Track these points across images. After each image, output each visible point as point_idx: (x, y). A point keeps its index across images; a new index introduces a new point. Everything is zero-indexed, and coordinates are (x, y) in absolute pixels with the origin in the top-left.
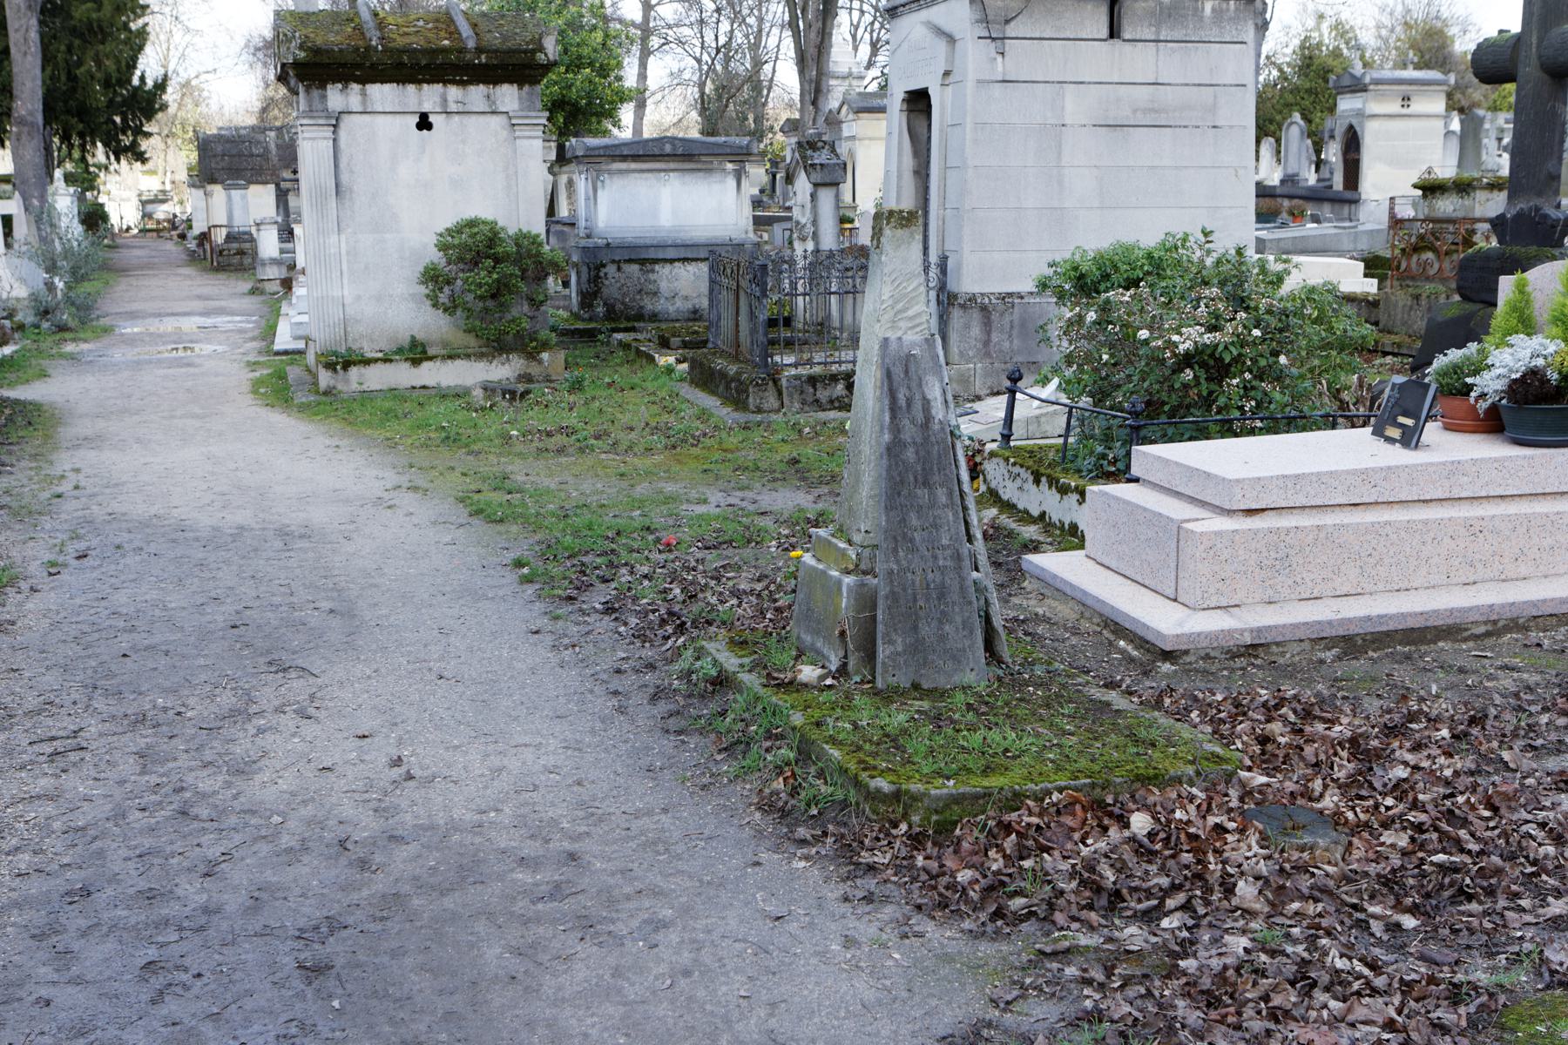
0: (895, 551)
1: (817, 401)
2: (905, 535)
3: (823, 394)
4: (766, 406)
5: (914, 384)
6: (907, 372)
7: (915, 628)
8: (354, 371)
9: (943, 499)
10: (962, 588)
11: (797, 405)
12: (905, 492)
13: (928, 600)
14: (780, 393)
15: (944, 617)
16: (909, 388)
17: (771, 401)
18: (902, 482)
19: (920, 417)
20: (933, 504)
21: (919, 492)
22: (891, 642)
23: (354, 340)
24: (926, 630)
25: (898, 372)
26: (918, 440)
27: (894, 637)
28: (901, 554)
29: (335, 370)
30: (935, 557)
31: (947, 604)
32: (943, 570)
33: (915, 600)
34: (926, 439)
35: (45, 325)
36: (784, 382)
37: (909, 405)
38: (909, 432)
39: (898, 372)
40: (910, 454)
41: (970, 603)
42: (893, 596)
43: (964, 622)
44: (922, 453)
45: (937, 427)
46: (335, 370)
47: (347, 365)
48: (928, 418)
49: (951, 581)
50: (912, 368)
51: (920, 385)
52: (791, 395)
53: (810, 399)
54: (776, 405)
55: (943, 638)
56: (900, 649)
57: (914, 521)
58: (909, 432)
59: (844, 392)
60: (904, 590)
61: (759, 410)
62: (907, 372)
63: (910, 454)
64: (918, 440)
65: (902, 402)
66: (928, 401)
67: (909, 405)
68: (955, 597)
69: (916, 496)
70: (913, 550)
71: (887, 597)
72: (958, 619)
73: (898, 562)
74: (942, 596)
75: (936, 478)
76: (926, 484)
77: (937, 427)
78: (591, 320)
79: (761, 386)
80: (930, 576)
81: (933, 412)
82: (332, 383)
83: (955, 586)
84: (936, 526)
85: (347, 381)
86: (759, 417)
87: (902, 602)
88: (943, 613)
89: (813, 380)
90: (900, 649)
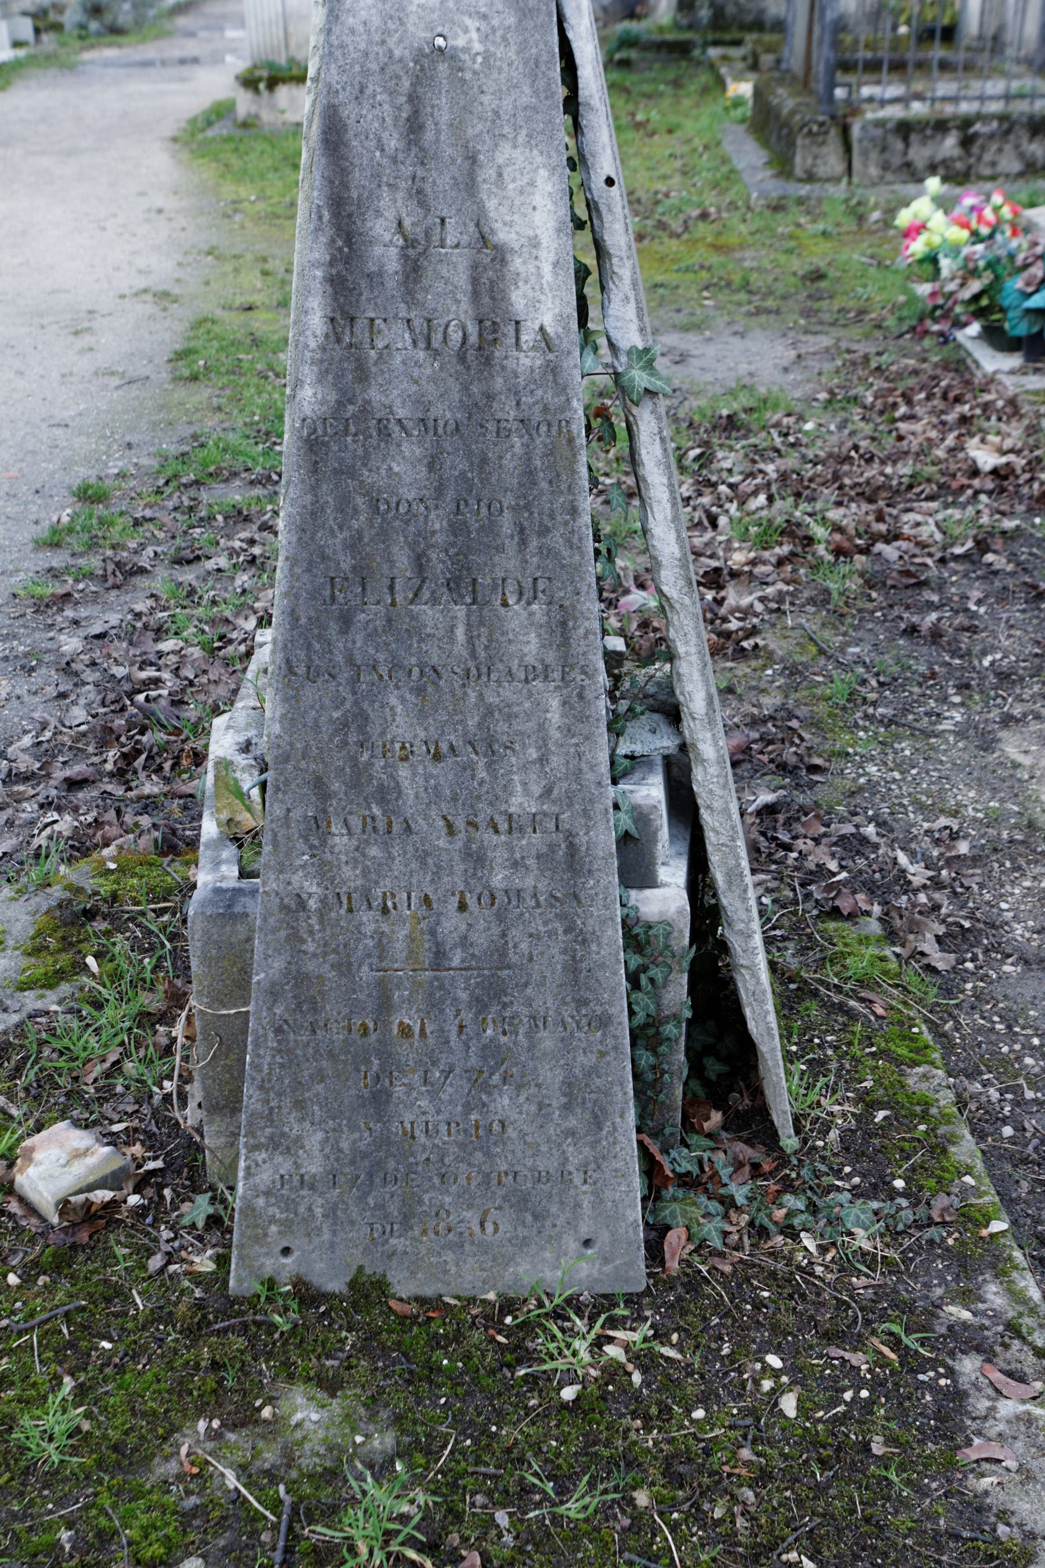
0: (317, 828)
1: (908, 165)
2: (358, 776)
3: (919, 154)
4: (821, 171)
5: (441, 181)
6: (414, 127)
7: (379, 1100)
8: (283, 92)
9: (530, 646)
10: (577, 972)
11: (874, 171)
12: (373, 613)
13: (434, 1007)
14: (848, 148)
15: (494, 1067)
16: (419, 196)
17: (832, 161)
18: (363, 576)
19: (458, 316)
20: (481, 667)
21: (429, 614)
22: (278, 1144)
23: (299, 46)
24: (415, 1107)
25: (376, 125)
26: (444, 412)
27: (293, 1127)
28: (340, 841)
29: (257, 90)
30: (477, 859)
31: (508, 1025)
32: (502, 905)
33: (385, 1005)
34: (477, 409)
35: (94, 26)
36: (856, 131)
37: (413, 269)
38: (406, 378)
39: (376, 125)
40: (403, 468)
41: (604, 1022)
42: (301, 991)
43: (569, 1087)
44: (455, 464)
45: (526, 361)
46: (257, 90)
47: (273, 83)
48: (493, 324)
49: (538, 948)
50: (442, 110)
51: (470, 186)
52: (865, 154)
53: (896, 161)
54: (839, 167)
55: (484, 1137)
56: (314, 1167)
57: (400, 719)
58: (406, 378)
59: (957, 152)
60: (345, 968)
61: (810, 177)
62: (414, 127)
63: (403, 468)
64: (444, 412)
65: (385, 252)
66: (500, 255)
67: (413, 269)
68: (546, 1001)
69: (417, 631)
70: (391, 826)
71: (274, 993)
72: (551, 1076)
73: (324, 871)
74: (491, 994)
75: (507, 562)
76: (462, 583)
77: (526, 361)
78: (690, 27)
79: (817, 137)
80: (452, 924)
81: (518, 299)
82: (253, 109)
83: (553, 956)
84: (491, 748)
85: (273, 107)
86: (804, 190)
87: (332, 1009)
88: (494, 1054)
89: (905, 129)
90: (314, 1167)
